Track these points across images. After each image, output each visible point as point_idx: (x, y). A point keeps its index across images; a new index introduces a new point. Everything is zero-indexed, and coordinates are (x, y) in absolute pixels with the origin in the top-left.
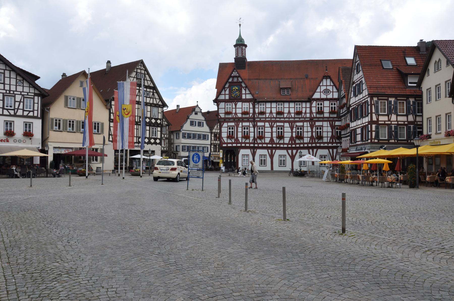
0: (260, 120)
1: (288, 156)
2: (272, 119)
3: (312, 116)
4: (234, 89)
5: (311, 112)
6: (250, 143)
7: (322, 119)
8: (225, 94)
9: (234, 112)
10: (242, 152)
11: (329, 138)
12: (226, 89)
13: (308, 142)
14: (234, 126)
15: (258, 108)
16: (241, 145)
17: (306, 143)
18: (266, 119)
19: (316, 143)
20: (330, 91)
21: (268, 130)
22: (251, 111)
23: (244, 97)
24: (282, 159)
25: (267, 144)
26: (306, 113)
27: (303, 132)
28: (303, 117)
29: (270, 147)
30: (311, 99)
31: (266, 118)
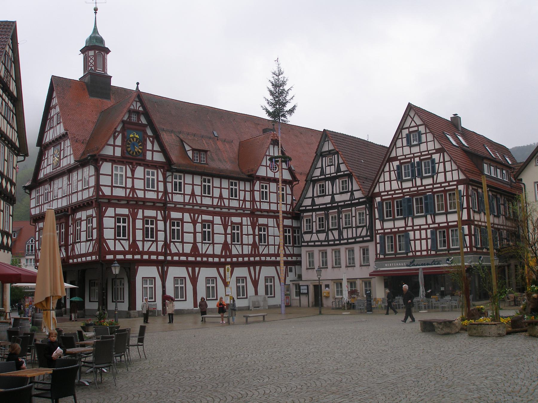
1: (219, 280)
2: (195, 207)
3: (255, 207)
4: (133, 138)
5: (253, 201)
6: (157, 253)
7: (266, 214)
8: (114, 146)
9: (129, 185)
10: (143, 272)
12: (117, 134)
13: (250, 253)
14: (127, 216)
15: (172, 182)
16: (142, 257)
17: (246, 256)
18: (184, 205)
21: (189, 227)
22: (161, 188)
23: (149, 156)
24: (211, 285)
25: (187, 255)
26: (244, 200)
27: (242, 235)
30: (253, 177)
31: (184, 204)
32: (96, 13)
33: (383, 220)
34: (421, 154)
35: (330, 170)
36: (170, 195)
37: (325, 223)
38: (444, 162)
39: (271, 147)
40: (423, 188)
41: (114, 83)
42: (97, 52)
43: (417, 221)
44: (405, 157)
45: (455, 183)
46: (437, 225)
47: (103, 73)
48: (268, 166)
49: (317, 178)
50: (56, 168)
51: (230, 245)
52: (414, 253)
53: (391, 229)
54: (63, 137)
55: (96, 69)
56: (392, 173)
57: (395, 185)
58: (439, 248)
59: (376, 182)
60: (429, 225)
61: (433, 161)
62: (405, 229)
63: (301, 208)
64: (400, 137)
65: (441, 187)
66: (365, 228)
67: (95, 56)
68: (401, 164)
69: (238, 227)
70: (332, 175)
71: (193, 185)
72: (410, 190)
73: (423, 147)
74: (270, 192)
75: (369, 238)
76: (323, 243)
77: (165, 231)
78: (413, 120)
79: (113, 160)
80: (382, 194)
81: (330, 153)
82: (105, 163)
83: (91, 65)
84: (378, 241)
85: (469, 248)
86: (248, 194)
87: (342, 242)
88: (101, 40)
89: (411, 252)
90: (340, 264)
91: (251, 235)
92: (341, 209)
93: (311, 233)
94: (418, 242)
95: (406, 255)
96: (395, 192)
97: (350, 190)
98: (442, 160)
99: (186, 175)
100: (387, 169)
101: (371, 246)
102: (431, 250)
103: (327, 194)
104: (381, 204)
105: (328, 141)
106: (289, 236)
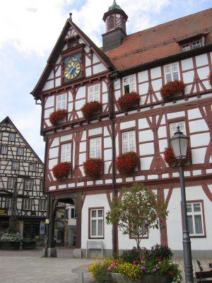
16: (86, 184)
23: (88, 73)
25: (146, 173)
29: (153, 182)
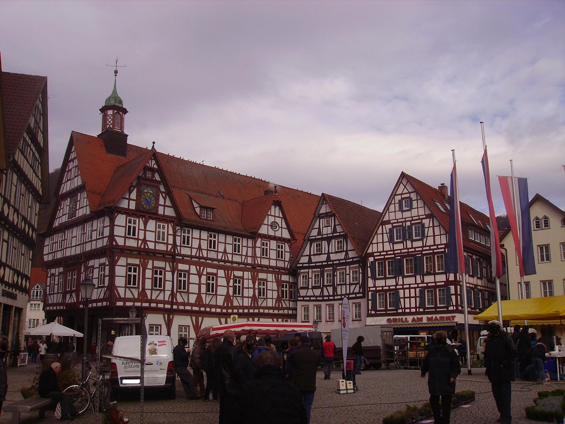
0: (183, 258)
3: (256, 263)
5: (254, 256)
6: (164, 302)
8: (129, 199)
9: (141, 237)
11: (274, 300)
13: (249, 305)
15: (181, 236)
16: (150, 305)
19: (259, 308)
20: (279, 226)
21: (194, 279)
22: (171, 241)
23: (161, 211)
25: (192, 305)
26: (247, 256)
28: (243, 261)
31: (191, 257)
32: (116, 75)
33: (374, 279)
34: (412, 218)
35: (327, 231)
36: (179, 248)
37: (321, 279)
38: (433, 227)
39: (273, 207)
40: (413, 250)
41: (130, 141)
42: (115, 111)
43: (408, 281)
44: (397, 221)
45: (444, 246)
46: (425, 285)
47: (120, 131)
48: (269, 225)
49: (314, 237)
50: (72, 218)
51: (232, 297)
52: (403, 310)
53: (382, 287)
54: (80, 189)
55: (114, 127)
56: (385, 235)
57: (387, 247)
58: (427, 306)
59: (369, 243)
60: (418, 284)
61: (423, 225)
62: (396, 287)
63: (298, 265)
64: (393, 202)
65: (430, 250)
66: (358, 285)
67: (114, 115)
68: (393, 227)
69: (239, 281)
70: (328, 235)
71: (200, 239)
72: (401, 251)
73: (414, 212)
74: (270, 249)
75: (361, 295)
76: (318, 298)
77: (173, 281)
78: (405, 187)
79: (127, 212)
80: (375, 254)
81: (326, 215)
82: (120, 215)
83: (110, 124)
84: (370, 298)
85: (455, 307)
86: (250, 250)
87: (336, 298)
88: (121, 102)
89: (400, 309)
90: (333, 318)
91: (251, 288)
92: (336, 267)
93: (307, 288)
94: (407, 300)
95: (396, 312)
96: (387, 253)
97: (345, 250)
98: (431, 225)
99: (194, 230)
100: (380, 231)
101: (363, 302)
102: (419, 308)
103: (323, 252)
104: (373, 263)
105: (326, 204)
106: (286, 291)
